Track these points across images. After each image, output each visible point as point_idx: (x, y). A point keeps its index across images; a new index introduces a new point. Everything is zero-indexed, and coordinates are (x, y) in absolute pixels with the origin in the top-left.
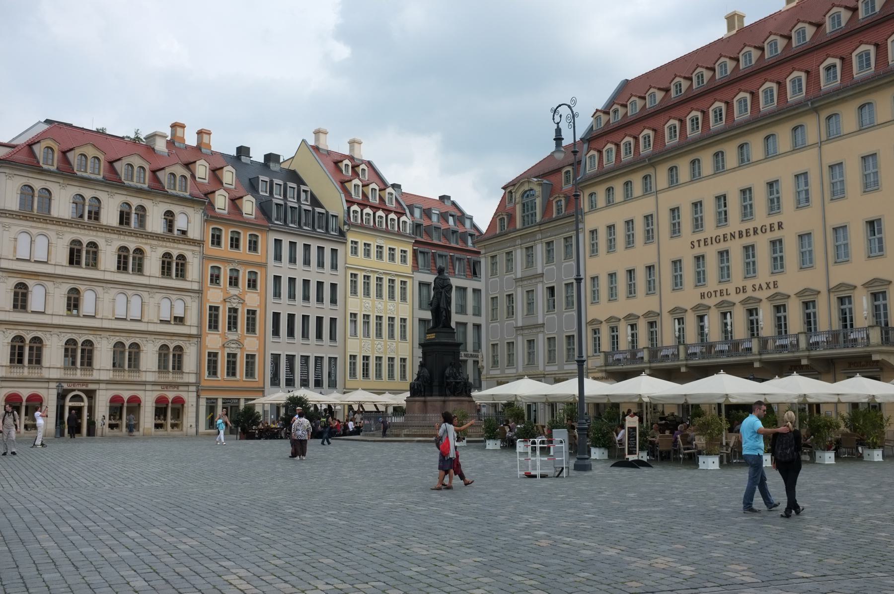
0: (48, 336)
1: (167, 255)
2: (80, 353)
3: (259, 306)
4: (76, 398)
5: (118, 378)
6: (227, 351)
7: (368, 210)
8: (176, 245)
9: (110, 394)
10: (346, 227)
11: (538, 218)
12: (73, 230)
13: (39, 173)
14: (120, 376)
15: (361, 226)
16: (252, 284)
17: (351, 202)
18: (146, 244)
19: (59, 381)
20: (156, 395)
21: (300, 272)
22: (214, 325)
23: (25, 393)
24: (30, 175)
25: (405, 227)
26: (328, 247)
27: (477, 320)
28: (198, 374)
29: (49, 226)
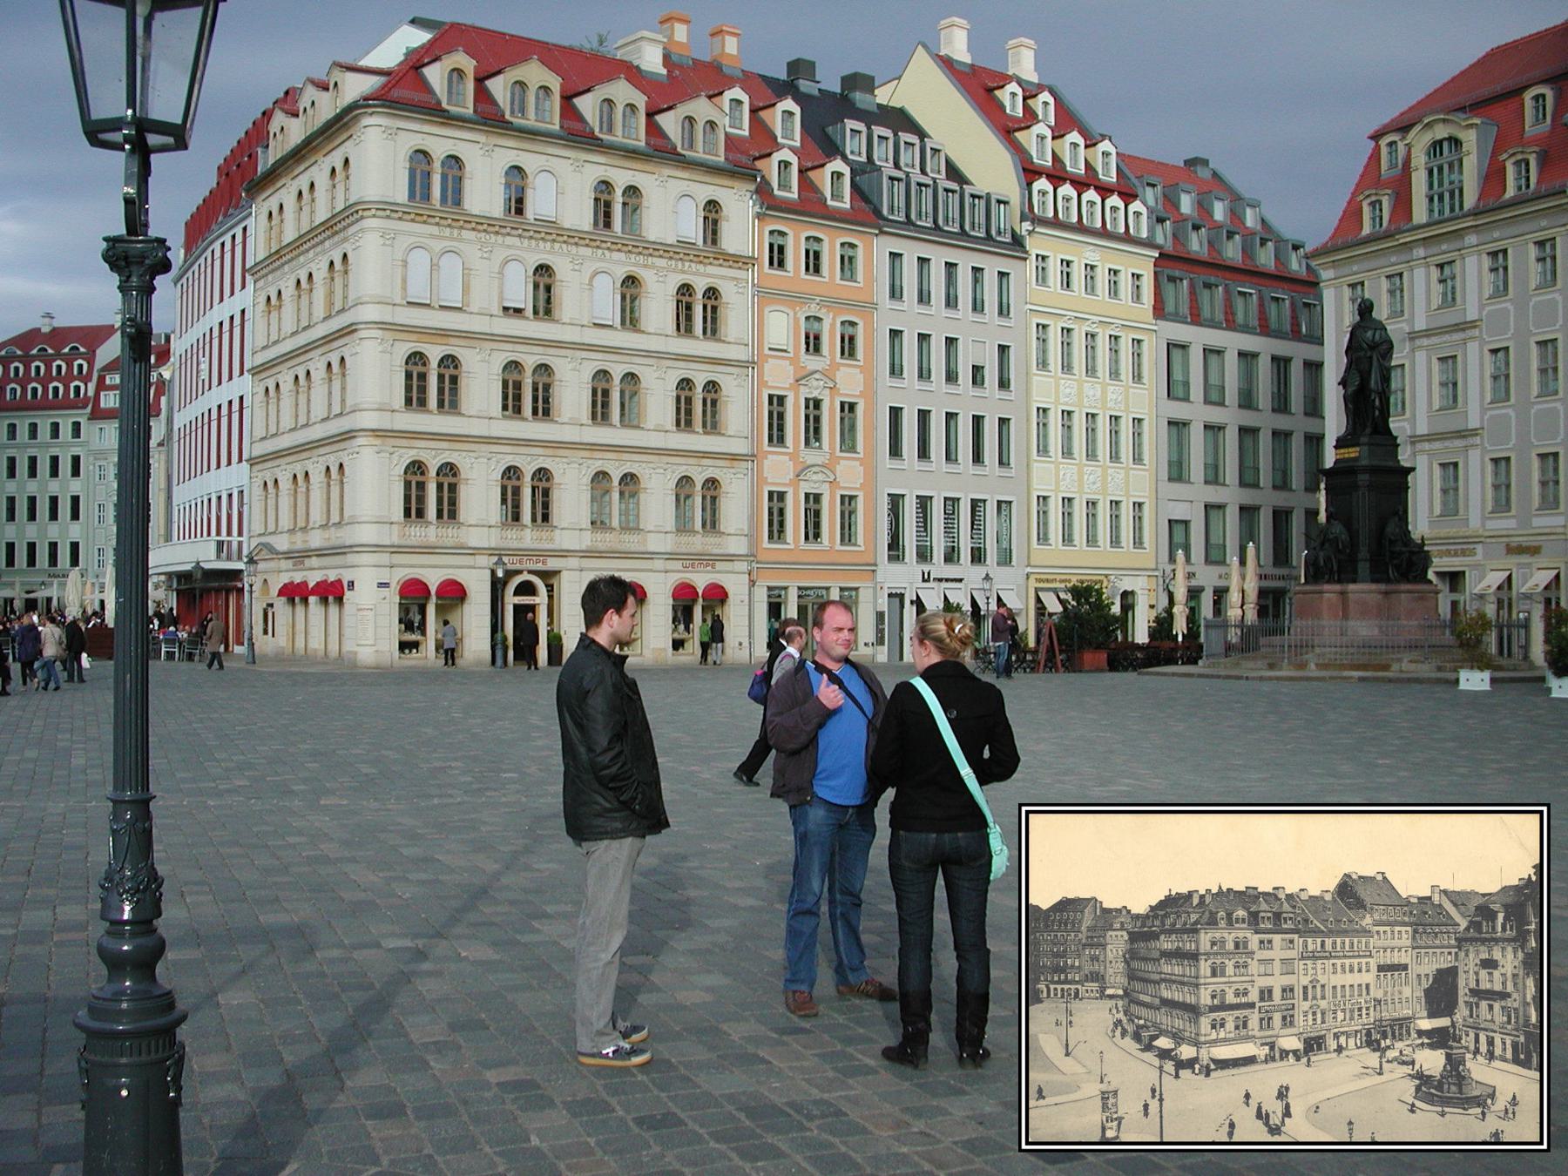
1: (685, 289)
2: (526, 497)
3: (862, 395)
5: (601, 547)
7: (1067, 190)
8: (701, 268)
10: (1027, 226)
11: (1470, 200)
12: (509, 240)
14: (605, 540)
15: (1055, 223)
16: (848, 346)
17: (1030, 173)
18: (645, 266)
19: (491, 552)
20: (674, 579)
21: (938, 321)
22: (777, 434)
23: (433, 580)
25: (1137, 224)
26: (992, 266)
27: (1282, 422)
28: (752, 537)
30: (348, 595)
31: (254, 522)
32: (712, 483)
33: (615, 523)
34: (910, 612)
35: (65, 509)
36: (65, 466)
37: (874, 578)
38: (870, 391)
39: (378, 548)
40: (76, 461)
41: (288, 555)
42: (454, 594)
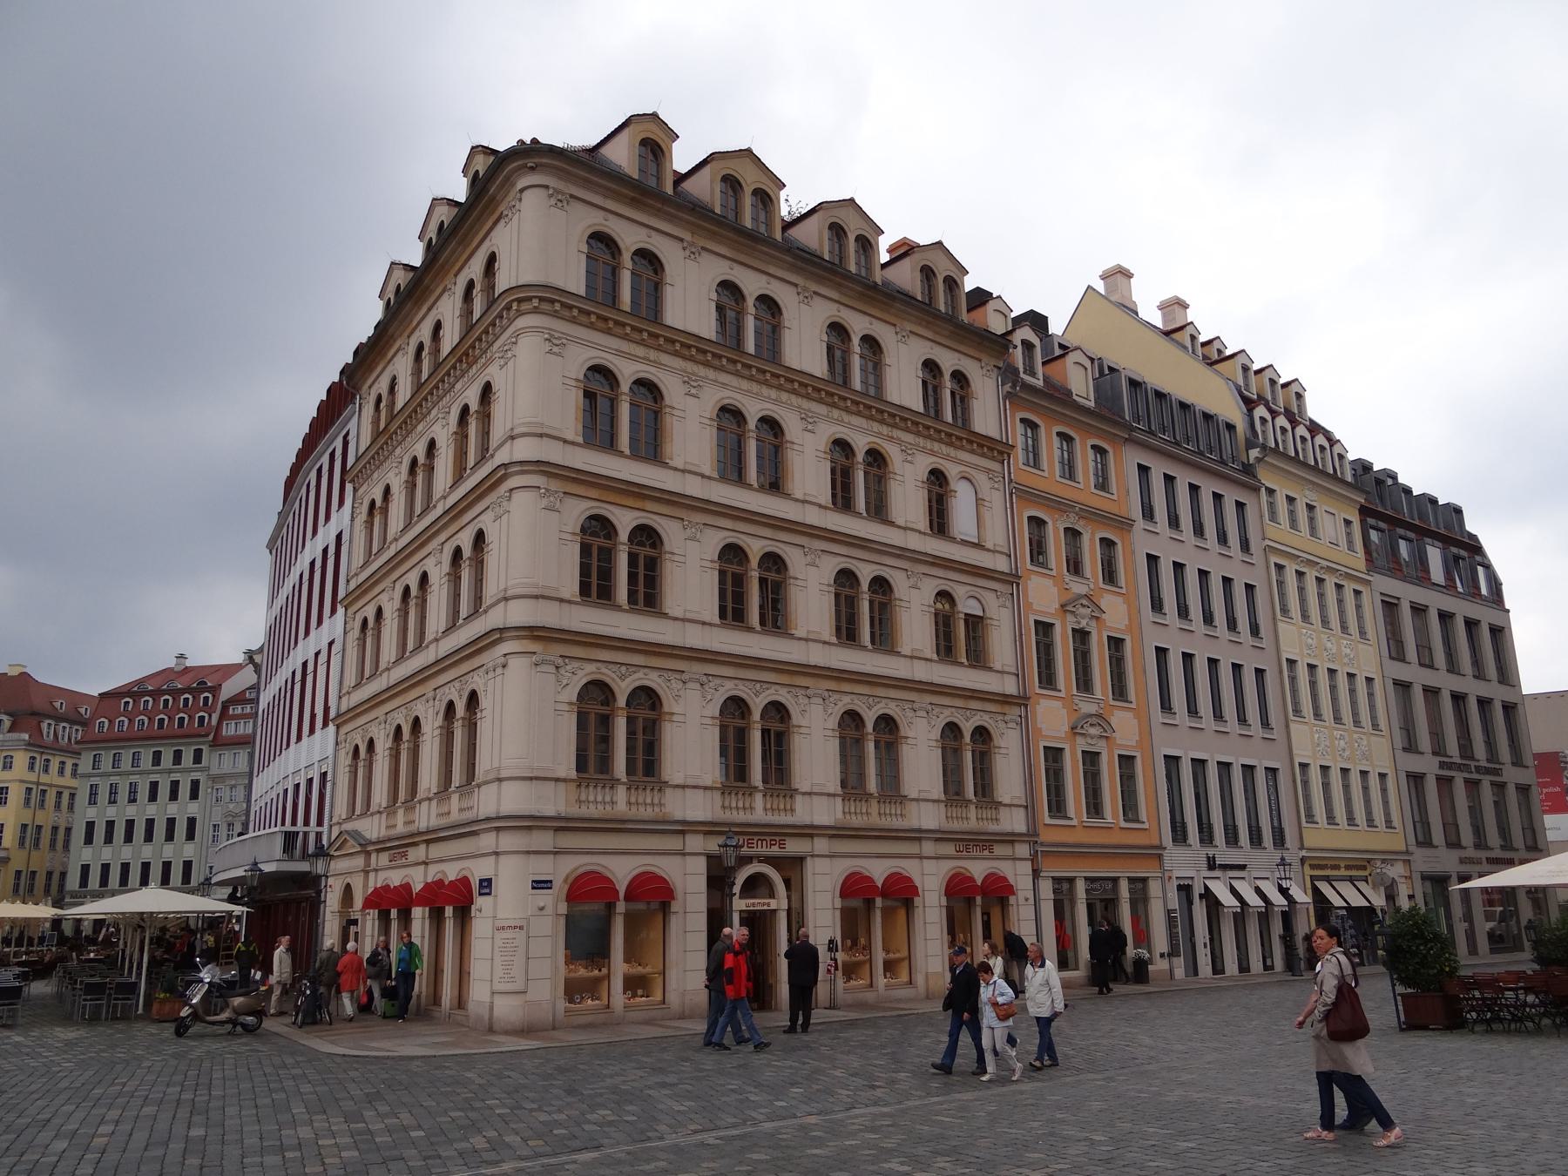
0: (676, 685)
2: (755, 743)
4: (755, 885)
5: (856, 821)
6: (1082, 744)
9: (842, 868)
13: (634, 203)
18: (891, 439)
19: (709, 829)
23: (622, 871)
24: (610, 204)
26: (1231, 496)
28: (1030, 808)
29: (666, 359)
30: (480, 902)
31: (339, 804)
32: (982, 733)
33: (872, 785)
34: (1200, 911)
35: (181, 830)
36: (184, 791)
37: (1161, 865)
38: (1135, 624)
39: (529, 823)
40: (195, 785)
41: (382, 846)
42: (653, 895)
